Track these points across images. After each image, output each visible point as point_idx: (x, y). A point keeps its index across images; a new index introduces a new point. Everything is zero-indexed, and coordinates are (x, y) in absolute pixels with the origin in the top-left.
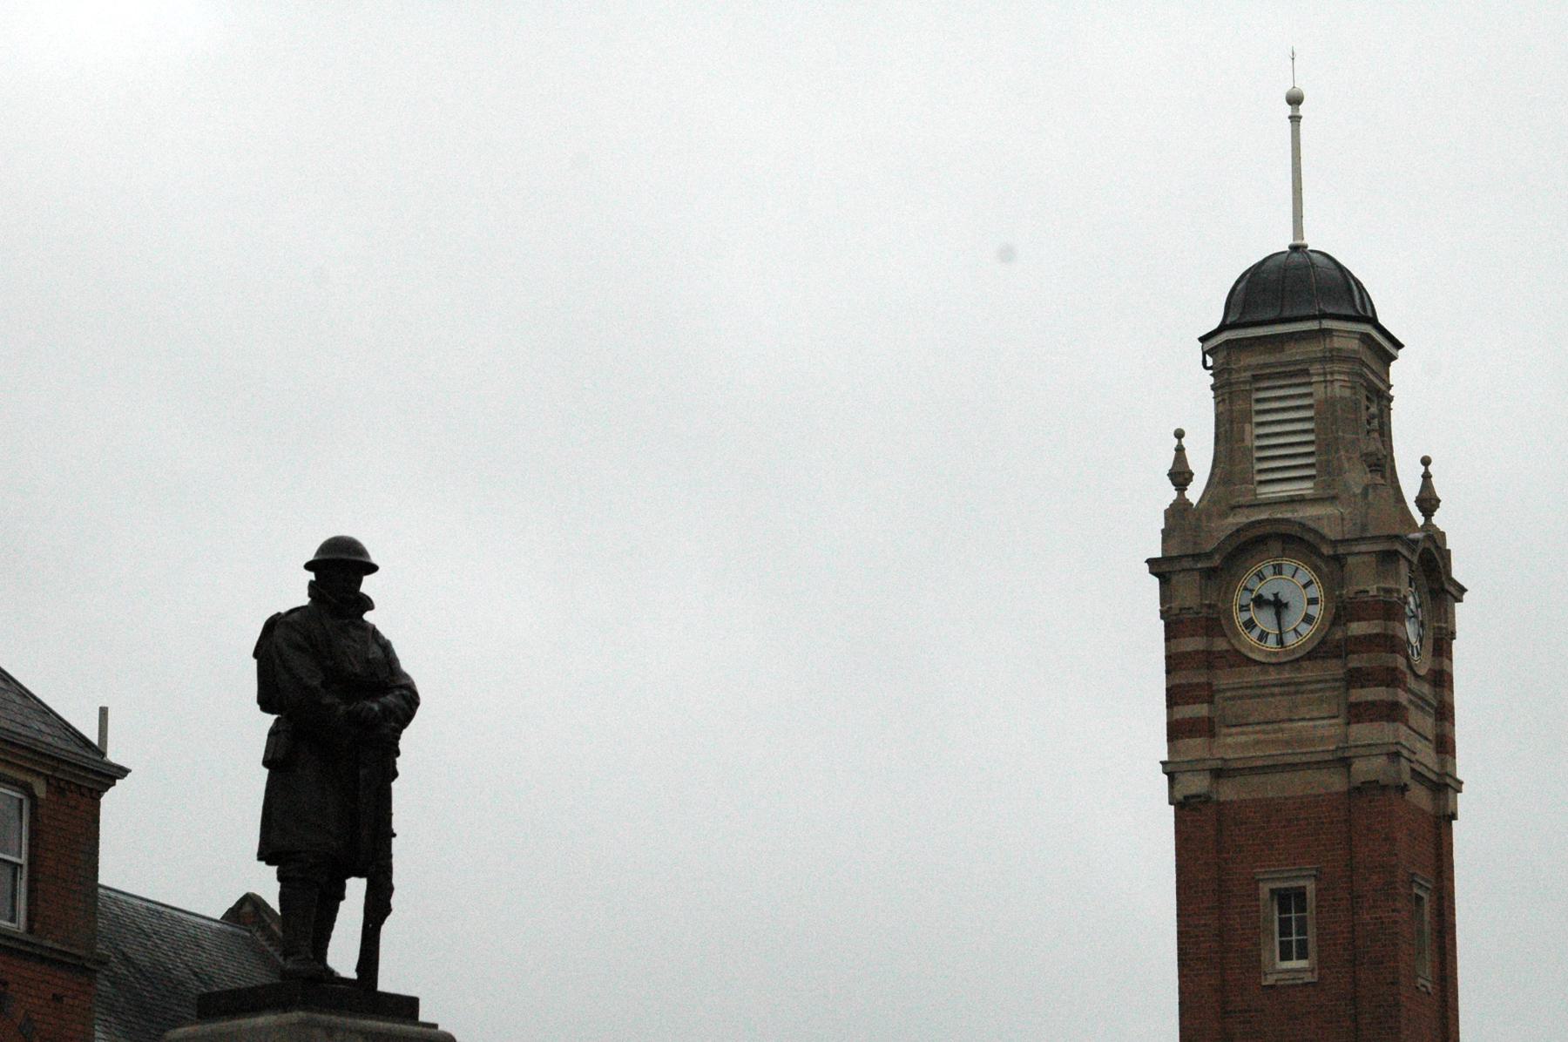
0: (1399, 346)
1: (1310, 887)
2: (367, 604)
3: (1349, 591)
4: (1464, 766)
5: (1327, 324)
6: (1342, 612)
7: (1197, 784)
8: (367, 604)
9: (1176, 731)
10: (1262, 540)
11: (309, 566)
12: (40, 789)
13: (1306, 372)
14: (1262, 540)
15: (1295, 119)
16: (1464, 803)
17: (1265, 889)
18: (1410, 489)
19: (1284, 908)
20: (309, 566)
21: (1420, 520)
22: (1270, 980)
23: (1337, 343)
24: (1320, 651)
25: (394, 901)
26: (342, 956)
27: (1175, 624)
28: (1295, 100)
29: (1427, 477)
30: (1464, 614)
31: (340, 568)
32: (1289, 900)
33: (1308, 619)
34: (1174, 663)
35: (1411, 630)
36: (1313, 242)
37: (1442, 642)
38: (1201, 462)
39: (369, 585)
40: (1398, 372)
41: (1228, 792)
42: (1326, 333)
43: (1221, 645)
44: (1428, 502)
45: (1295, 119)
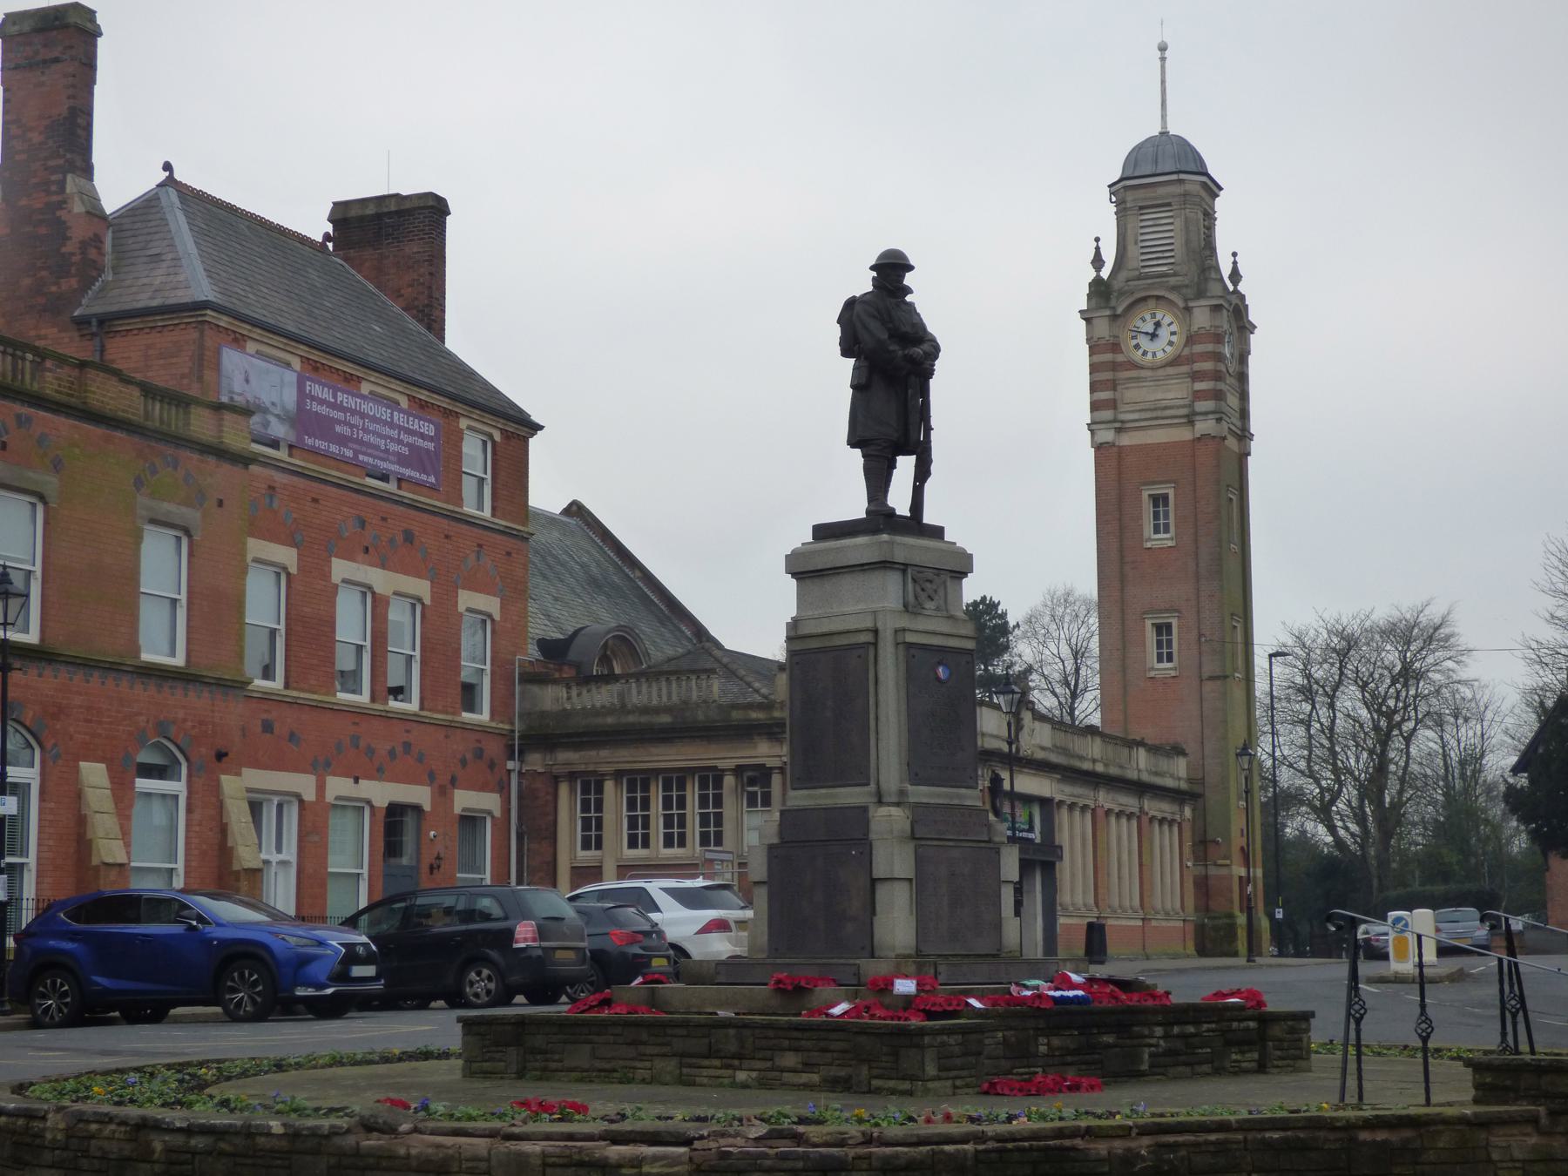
0: (1221, 189)
1: (1171, 493)
2: (908, 291)
3: (1195, 328)
4: (1255, 426)
5: (1182, 176)
6: (1190, 340)
7: (1107, 436)
8: (908, 291)
9: (1095, 406)
10: (1145, 299)
11: (873, 268)
12: (497, 436)
13: (1169, 204)
14: (1145, 299)
15: (1163, 59)
16: (1255, 446)
17: (1145, 494)
18: (1226, 270)
19: (1156, 505)
20: (873, 268)
21: (1231, 288)
22: (1149, 545)
23: (1188, 187)
24: (1175, 362)
25: (933, 468)
26: (899, 499)
27: (1094, 347)
28: (1163, 48)
29: (1235, 263)
30: (1255, 340)
31: (891, 270)
32: (1159, 501)
33: (1171, 343)
34: (1093, 368)
35: (1227, 351)
36: (1173, 131)
37: (1243, 357)
38: (1109, 257)
39: (909, 279)
40: (1220, 204)
41: (1126, 440)
42: (1181, 181)
43: (1120, 358)
44: (1236, 276)
45: (1163, 59)
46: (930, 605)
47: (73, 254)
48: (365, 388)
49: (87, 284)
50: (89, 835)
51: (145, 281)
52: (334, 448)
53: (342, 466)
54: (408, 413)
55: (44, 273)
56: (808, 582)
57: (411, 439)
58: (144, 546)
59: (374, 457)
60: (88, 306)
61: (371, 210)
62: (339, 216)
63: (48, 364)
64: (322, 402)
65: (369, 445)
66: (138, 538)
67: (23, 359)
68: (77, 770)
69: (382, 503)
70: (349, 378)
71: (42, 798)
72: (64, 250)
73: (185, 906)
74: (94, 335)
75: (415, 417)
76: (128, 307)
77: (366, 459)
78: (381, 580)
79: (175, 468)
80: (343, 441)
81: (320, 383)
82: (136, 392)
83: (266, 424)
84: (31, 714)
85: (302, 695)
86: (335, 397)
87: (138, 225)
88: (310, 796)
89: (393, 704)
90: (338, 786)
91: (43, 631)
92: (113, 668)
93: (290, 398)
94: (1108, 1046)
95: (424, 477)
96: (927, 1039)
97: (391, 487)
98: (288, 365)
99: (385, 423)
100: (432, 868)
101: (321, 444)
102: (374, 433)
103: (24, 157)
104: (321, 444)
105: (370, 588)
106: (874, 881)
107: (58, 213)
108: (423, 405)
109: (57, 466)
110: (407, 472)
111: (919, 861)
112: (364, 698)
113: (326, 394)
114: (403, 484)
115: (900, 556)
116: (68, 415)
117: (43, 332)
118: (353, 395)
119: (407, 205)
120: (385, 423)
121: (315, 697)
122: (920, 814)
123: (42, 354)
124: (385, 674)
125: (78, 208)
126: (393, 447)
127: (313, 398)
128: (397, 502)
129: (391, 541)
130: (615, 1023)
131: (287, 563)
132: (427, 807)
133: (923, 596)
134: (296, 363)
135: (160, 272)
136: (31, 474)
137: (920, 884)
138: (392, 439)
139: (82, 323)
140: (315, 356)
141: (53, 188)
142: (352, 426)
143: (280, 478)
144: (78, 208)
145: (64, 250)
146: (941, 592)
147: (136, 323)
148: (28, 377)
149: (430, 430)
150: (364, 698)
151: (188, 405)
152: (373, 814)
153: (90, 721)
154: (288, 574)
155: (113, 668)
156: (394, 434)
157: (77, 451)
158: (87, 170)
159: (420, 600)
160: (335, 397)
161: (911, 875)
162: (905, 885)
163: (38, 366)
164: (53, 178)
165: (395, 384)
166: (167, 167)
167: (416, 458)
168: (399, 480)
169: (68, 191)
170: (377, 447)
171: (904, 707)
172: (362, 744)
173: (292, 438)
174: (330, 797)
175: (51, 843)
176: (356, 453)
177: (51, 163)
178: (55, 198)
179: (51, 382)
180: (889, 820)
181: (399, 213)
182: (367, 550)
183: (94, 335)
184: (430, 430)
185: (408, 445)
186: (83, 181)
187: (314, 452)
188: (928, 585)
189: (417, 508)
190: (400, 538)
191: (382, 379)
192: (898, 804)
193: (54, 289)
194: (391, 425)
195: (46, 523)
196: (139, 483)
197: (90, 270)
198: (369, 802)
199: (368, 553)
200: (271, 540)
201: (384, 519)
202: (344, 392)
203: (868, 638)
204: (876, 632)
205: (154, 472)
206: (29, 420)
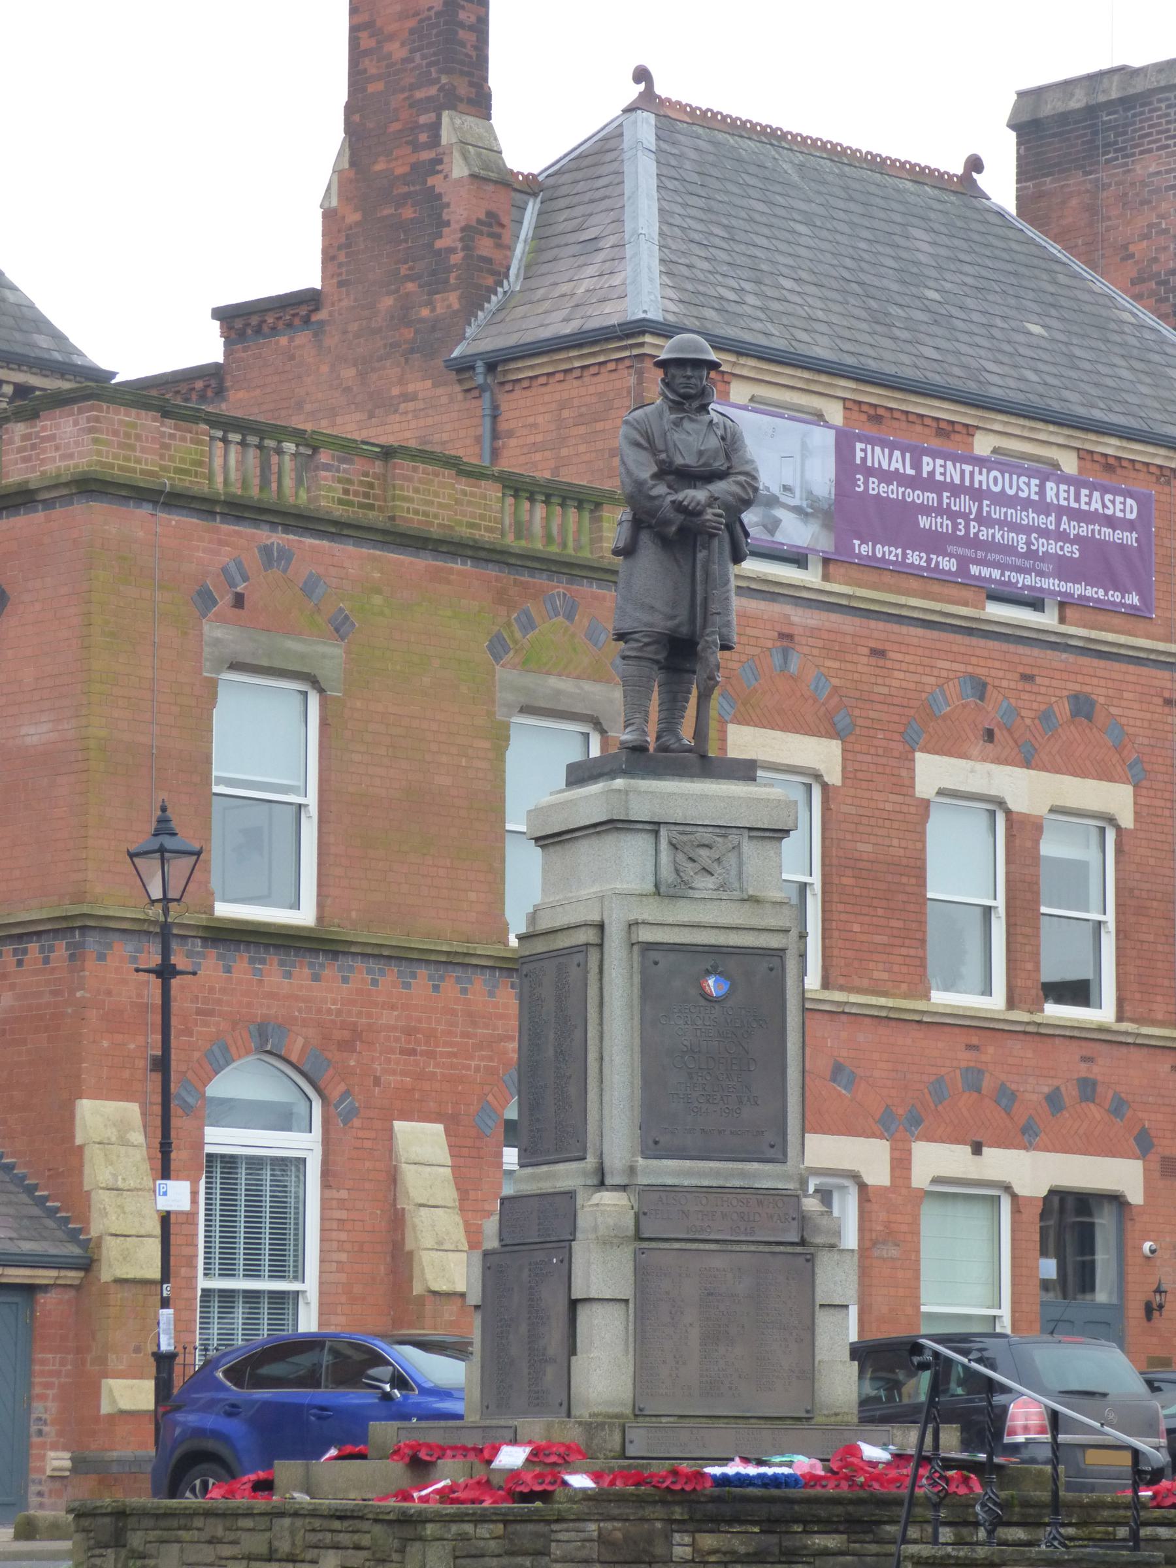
46: (704, 884)
47: (451, 250)
48: (983, 445)
49: (474, 301)
50: (409, 1245)
51: (565, 288)
52: (915, 558)
53: (936, 588)
54: (1077, 483)
55: (411, 286)
56: (551, 849)
57: (1084, 530)
58: (510, 755)
59: (1003, 567)
60: (478, 339)
61: (1077, 102)
62: (1026, 118)
63: (324, 457)
64: (887, 477)
65: (991, 546)
66: (500, 739)
67: (280, 452)
68: (390, 1132)
69: (1021, 649)
70: (945, 430)
71: (326, 1184)
72: (439, 244)
73: (378, 1360)
74: (482, 389)
75: (1093, 487)
76: (528, 338)
77: (986, 572)
78: (1024, 788)
79: (570, 617)
80: (935, 543)
81: (883, 444)
82: (493, 491)
83: (773, 526)
84: (300, 1041)
85: (853, 998)
86: (917, 465)
87: (581, 187)
88: (878, 1175)
89: (1055, 1011)
90: (934, 1160)
91: (321, 906)
92: (454, 962)
93: (821, 475)
94: (825, 1553)
95: (1115, 596)
96: (430, 1529)
97: (1047, 620)
98: (819, 418)
99: (1027, 504)
100: (1150, 1310)
101: (892, 553)
102: (1003, 524)
103: (379, 86)
104: (892, 553)
105: (1001, 803)
106: (574, 1304)
107: (430, 181)
108: (1110, 465)
109: (340, 627)
110: (1078, 590)
111: (641, 1273)
112: (995, 1002)
113: (898, 463)
114: (1069, 612)
115: (640, 810)
116: (359, 541)
117: (411, 388)
118: (955, 459)
119: (1139, 86)
120: (1027, 504)
121: (882, 1001)
122: (652, 1201)
123: (311, 443)
124: (1036, 956)
125: (459, 170)
126: (1043, 546)
127: (869, 472)
128: (1054, 646)
129: (1046, 717)
130: (208, 1514)
131: (822, 768)
132: (1136, 1197)
133: (689, 868)
134: (835, 414)
135: (591, 270)
136: (291, 645)
137: (645, 1307)
138: (1044, 533)
139: (463, 368)
140: (872, 396)
141: (423, 137)
142: (953, 516)
143: (800, 618)
144: (459, 170)
145: (439, 244)
146: (732, 859)
147: (541, 365)
148: (288, 483)
149: (1129, 509)
150: (995, 1002)
151: (598, 505)
152: (1016, 1210)
153: (413, 1052)
154: (825, 787)
155: (454, 962)
156: (1050, 522)
157: (377, 600)
158: (481, 103)
159: (1111, 820)
160: (917, 465)
161: (627, 1292)
162: (617, 1311)
163: (307, 463)
164: (423, 119)
165: (1047, 432)
166: (642, 75)
167: (1098, 562)
168: (1062, 605)
169: (444, 141)
170: (1011, 550)
171: (637, 1041)
172: (987, 1084)
173: (826, 543)
174: (920, 1178)
175: (343, 1257)
176: (964, 563)
177: (419, 94)
178: (426, 155)
179: (327, 491)
180: (606, 1209)
181: (1126, 102)
182: (990, 735)
183: (482, 389)
184: (1129, 509)
185: (1077, 540)
186: (470, 122)
187: (874, 566)
188: (704, 852)
189: (1100, 655)
190: (1063, 709)
191: (1016, 425)
192: (624, 1188)
193: (425, 312)
194: (1043, 507)
195: (324, 724)
196: (498, 647)
197: (481, 278)
198: (1008, 1188)
199: (994, 741)
200: (785, 728)
201: (1027, 678)
202: (934, 455)
203: (589, 936)
204: (601, 927)
205: (528, 625)
206: (285, 555)
